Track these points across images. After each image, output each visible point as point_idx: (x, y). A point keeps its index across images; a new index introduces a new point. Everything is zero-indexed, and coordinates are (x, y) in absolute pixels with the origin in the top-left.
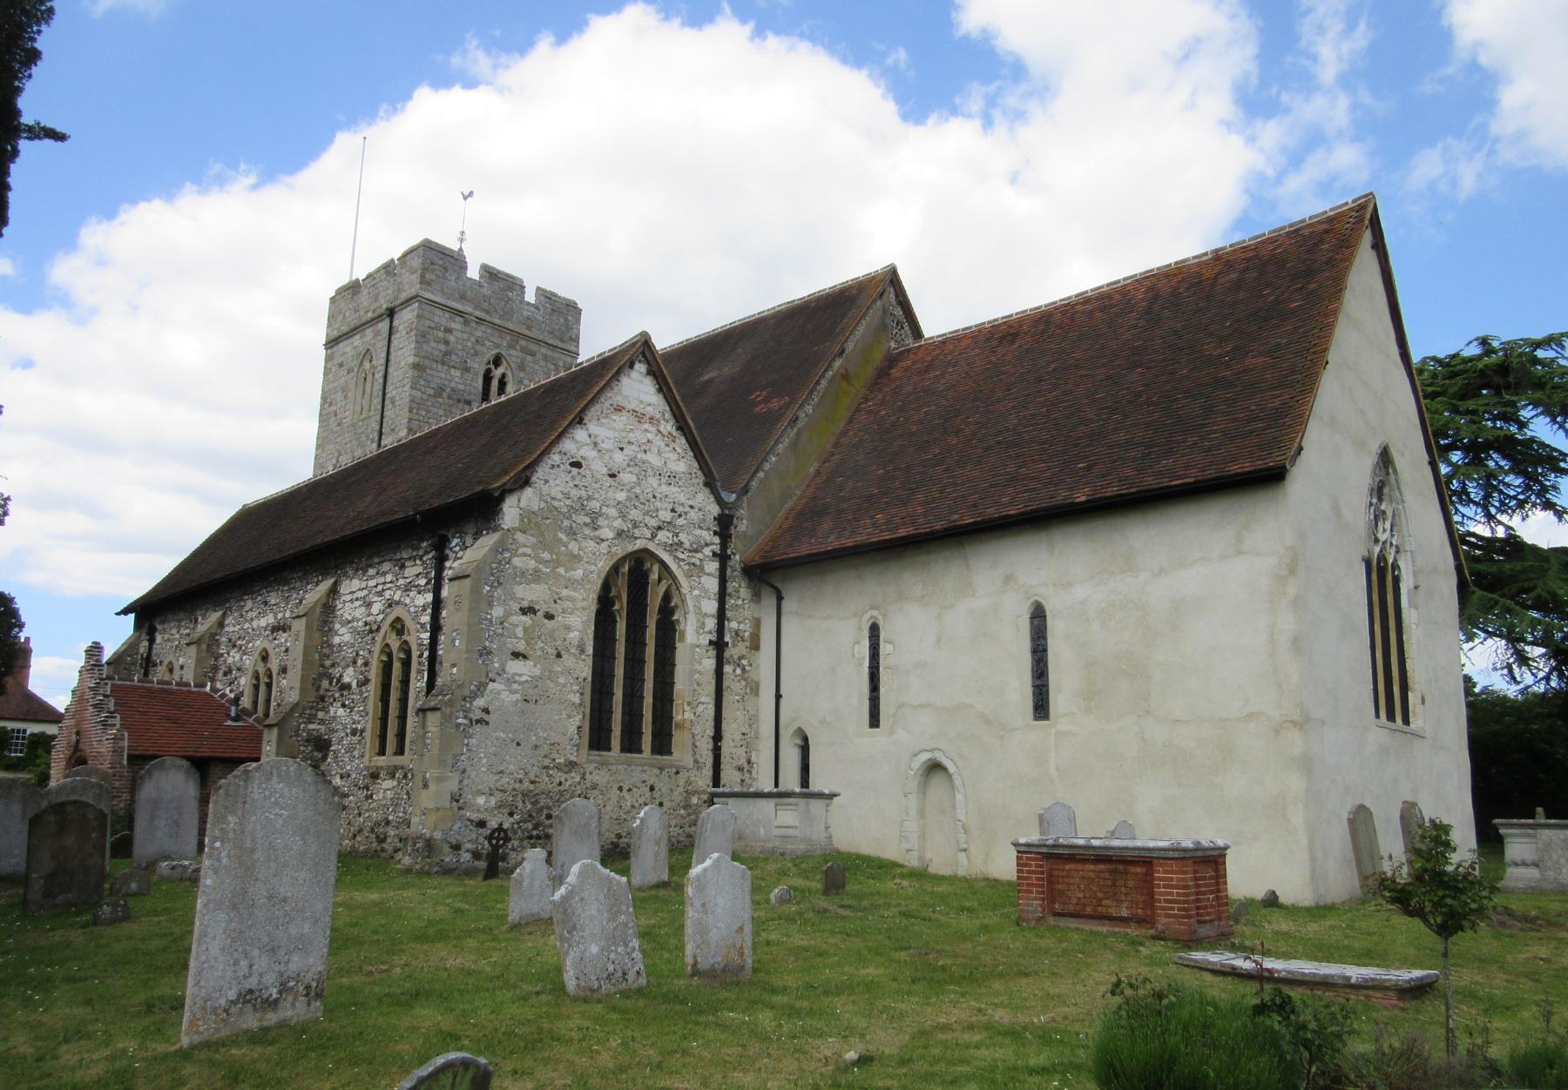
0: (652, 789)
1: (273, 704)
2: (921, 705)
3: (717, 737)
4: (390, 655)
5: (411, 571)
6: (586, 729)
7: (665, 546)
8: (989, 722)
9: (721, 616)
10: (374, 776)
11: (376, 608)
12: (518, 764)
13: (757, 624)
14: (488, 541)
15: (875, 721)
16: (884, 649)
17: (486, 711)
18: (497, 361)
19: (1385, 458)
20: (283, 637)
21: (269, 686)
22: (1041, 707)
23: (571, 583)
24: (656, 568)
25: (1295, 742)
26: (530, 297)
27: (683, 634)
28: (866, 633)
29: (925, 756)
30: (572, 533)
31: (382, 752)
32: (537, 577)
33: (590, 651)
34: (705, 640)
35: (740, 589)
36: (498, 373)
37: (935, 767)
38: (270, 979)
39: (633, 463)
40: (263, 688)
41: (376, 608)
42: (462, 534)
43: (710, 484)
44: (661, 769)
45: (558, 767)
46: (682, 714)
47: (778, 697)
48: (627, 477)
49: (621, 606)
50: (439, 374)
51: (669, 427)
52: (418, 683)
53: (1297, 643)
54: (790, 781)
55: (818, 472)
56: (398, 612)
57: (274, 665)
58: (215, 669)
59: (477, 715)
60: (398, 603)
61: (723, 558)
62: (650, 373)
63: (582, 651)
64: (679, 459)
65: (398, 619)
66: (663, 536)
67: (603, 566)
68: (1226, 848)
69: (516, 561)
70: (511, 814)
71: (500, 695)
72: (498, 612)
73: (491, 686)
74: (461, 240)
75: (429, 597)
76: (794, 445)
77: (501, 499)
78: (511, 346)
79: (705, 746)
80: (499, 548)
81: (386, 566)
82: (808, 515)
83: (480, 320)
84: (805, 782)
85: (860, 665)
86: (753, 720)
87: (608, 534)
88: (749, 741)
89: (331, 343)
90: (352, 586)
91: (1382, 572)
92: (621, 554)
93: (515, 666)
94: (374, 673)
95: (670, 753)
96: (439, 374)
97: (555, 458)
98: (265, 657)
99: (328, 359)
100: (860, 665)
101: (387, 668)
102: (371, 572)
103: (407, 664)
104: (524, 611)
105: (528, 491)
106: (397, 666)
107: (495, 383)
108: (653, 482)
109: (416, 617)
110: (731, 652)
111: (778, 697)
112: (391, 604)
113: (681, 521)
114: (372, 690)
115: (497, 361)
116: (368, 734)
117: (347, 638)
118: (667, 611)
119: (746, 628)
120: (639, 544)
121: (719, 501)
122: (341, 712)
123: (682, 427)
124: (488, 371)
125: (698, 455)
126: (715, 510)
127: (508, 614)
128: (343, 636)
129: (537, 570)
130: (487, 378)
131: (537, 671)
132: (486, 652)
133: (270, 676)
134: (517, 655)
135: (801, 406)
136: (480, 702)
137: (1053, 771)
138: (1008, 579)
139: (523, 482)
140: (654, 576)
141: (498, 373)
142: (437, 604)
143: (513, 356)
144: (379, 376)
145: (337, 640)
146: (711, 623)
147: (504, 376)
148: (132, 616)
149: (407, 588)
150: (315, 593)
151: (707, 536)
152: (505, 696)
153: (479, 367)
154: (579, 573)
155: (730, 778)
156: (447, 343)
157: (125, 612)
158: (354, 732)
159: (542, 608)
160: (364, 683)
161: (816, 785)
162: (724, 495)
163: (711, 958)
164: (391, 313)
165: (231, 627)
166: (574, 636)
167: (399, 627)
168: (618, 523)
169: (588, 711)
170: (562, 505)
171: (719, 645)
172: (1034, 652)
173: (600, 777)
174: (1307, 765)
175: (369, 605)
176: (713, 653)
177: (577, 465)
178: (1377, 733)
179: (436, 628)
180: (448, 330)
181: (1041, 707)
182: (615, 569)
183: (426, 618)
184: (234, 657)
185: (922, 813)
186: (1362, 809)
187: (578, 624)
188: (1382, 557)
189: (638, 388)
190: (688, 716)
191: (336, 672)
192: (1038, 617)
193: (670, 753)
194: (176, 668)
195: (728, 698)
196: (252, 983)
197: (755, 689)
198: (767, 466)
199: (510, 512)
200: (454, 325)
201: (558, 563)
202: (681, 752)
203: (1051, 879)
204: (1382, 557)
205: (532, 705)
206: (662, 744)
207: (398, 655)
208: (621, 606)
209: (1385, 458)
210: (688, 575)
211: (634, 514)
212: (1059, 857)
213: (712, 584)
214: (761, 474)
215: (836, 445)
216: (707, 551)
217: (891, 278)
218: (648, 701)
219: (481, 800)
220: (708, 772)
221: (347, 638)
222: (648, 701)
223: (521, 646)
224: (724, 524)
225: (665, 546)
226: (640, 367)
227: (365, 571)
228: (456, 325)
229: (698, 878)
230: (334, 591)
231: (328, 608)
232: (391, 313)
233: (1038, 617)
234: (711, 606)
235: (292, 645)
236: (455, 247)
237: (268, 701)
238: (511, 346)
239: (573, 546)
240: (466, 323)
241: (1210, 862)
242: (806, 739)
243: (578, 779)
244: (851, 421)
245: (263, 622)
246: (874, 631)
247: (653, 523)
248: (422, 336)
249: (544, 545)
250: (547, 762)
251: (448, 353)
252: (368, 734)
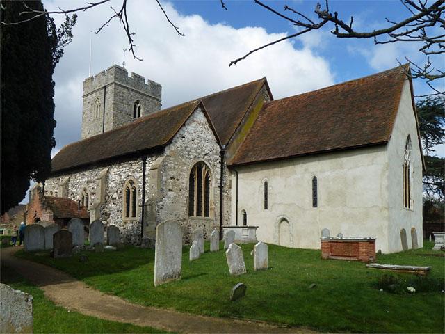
1: (89, 203)
3: (221, 212)
4: (129, 190)
5: (134, 167)
7: (209, 161)
8: (300, 208)
9: (222, 179)
13: (231, 181)
14: (160, 159)
15: (266, 208)
18: (138, 102)
19: (409, 138)
20: (91, 184)
21: (87, 198)
22: (315, 204)
25: (386, 213)
26: (147, 83)
29: (281, 217)
30: (183, 156)
31: (128, 216)
34: (217, 186)
35: (226, 171)
37: (284, 220)
38: (171, 271)
39: (198, 137)
40: (85, 199)
41: (123, 177)
42: (151, 156)
43: (218, 143)
45: (181, 220)
46: (211, 206)
47: (237, 201)
48: (197, 141)
49: (196, 176)
51: (207, 126)
52: (139, 198)
53: (388, 188)
54: (241, 223)
55: (246, 139)
56: (131, 178)
57: (89, 193)
58: (68, 193)
61: (222, 163)
64: (210, 136)
65: (131, 180)
67: (191, 165)
68: (375, 240)
72: (164, 178)
75: (142, 174)
77: (165, 147)
79: (218, 214)
80: (164, 161)
81: (126, 165)
83: (133, 90)
84: (245, 223)
85: (262, 193)
86: (230, 207)
87: (192, 157)
88: (229, 213)
89: (84, 96)
91: (406, 168)
93: (169, 193)
97: (178, 136)
98: (85, 190)
99: (84, 100)
100: (262, 193)
101: (128, 194)
102: (121, 167)
103: (135, 192)
104: (171, 178)
106: (131, 193)
109: (137, 180)
110: (225, 189)
111: (237, 201)
113: (211, 153)
114: (124, 199)
115: (138, 102)
116: (123, 212)
117: (114, 185)
118: (207, 178)
119: (228, 182)
120: (200, 160)
121: (221, 147)
123: (211, 127)
125: (215, 134)
126: (220, 150)
128: (112, 184)
131: (175, 195)
132: (162, 190)
133: (88, 195)
134: (170, 190)
136: (161, 203)
137: (318, 220)
138: (306, 170)
139: (170, 142)
140: (204, 168)
142: (144, 176)
143: (142, 101)
144: (102, 106)
146: (219, 181)
149: (133, 172)
150: (102, 172)
151: (218, 157)
153: (132, 104)
155: (225, 223)
158: (118, 211)
159: (176, 178)
161: (248, 225)
163: (261, 266)
164: (105, 87)
165: (72, 181)
166: (184, 185)
167: (131, 182)
168: (195, 154)
170: (180, 149)
171: (221, 187)
172: (313, 189)
173: (191, 223)
174: (389, 219)
175: (121, 176)
176: (219, 189)
177: (184, 137)
178: (403, 210)
179: (144, 183)
180: (123, 93)
181: (315, 204)
182: (194, 166)
183: (141, 180)
184: (74, 190)
185: (279, 232)
186: (404, 229)
187: (185, 182)
188: (406, 164)
189: (199, 116)
191: (111, 194)
192: (315, 180)
194: (54, 193)
195: (224, 202)
196: (168, 272)
197: (230, 199)
199: (167, 152)
201: (179, 165)
202: (211, 216)
203: (331, 246)
204: (406, 164)
206: (207, 214)
207: (131, 190)
209: (409, 138)
210: (213, 168)
212: (333, 242)
213: (219, 170)
216: (218, 161)
217: (264, 83)
218: (203, 202)
220: (219, 221)
222: (203, 202)
223: (171, 188)
224: (222, 154)
225: (209, 161)
226: (199, 109)
227: (118, 166)
228: (126, 91)
229: (257, 247)
230: (108, 172)
231: (107, 176)
232: (105, 87)
233: (315, 180)
234: (219, 176)
235: (97, 187)
237: (87, 202)
241: (372, 242)
242: (245, 212)
245: (84, 180)
246: (266, 183)
247: (204, 153)
248: (116, 95)
249: (176, 160)
250: (178, 219)
251: (123, 100)
252: (123, 212)
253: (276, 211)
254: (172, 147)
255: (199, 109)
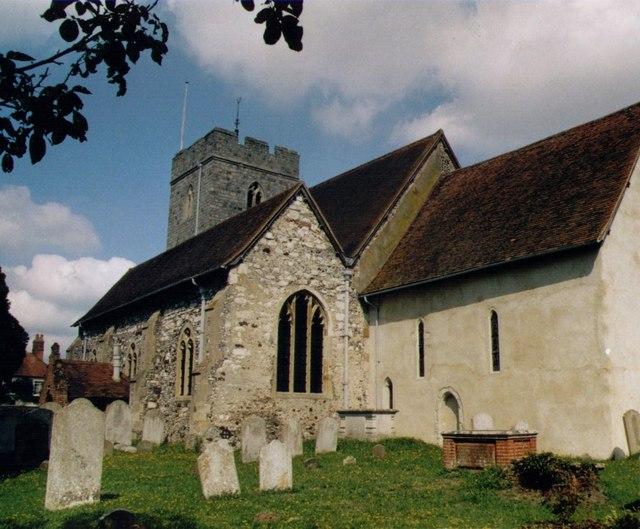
0: (311, 410)
2: (442, 365)
4: (184, 346)
6: (275, 380)
7: (319, 288)
10: (179, 406)
11: (179, 323)
12: (239, 399)
15: (422, 373)
16: (426, 336)
17: (223, 374)
18: (256, 185)
23: (265, 309)
24: (311, 298)
26: (272, 151)
27: (326, 331)
28: (417, 328)
29: (444, 391)
30: (265, 284)
32: (247, 306)
33: (276, 341)
36: (256, 192)
41: (179, 323)
44: (316, 400)
45: (260, 400)
49: (292, 319)
50: (225, 195)
51: (315, 227)
56: (187, 325)
59: (219, 376)
60: (187, 321)
62: (305, 201)
63: (272, 342)
65: (187, 329)
66: (313, 282)
67: (282, 299)
69: (237, 300)
70: (237, 423)
71: (229, 366)
72: (228, 325)
73: (226, 361)
74: (237, 124)
76: (386, 231)
78: (262, 178)
82: (390, 268)
83: (245, 166)
90: (170, 315)
92: (291, 293)
93: (237, 352)
94: (179, 352)
95: (320, 391)
96: (225, 195)
98: (133, 346)
99: (173, 190)
104: (241, 324)
105: (242, 266)
107: (254, 197)
108: (308, 255)
112: (185, 321)
114: (179, 363)
115: (256, 185)
117: (167, 338)
118: (317, 320)
120: (301, 288)
122: (165, 374)
124: (251, 192)
125: (331, 240)
127: (233, 326)
129: (247, 304)
130: (250, 195)
131: (249, 353)
132: (222, 345)
134: (238, 346)
135: (390, 211)
136: (220, 370)
140: (310, 303)
141: (256, 192)
143: (264, 183)
145: (163, 339)
147: (259, 193)
148: (77, 328)
152: (234, 367)
153: (245, 190)
154: (269, 304)
156: (228, 179)
157: (75, 325)
159: (251, 322)
160: (174, 360)
161: (395, 408)
162: (346, 259)
166: (267, 335)
168: (290, 278)
169: (276, 372)
173: (282, 405)
182: (289, 300)
187: (270, 329)
189: (299, 208)
190: (330, 372)
192: (495, 317)
193: (320, 391)
198: (371, 243)
200: (231, 170)
205: (246, 370)
206: (317, 387)
208: (292, 319)
210: (328, 301)
211: (300, 273)
214: (368, 247)
215: (411, 229)
219: (221, 417)
221: (167, 338)
223: (240, 342)
225: (319, 288)
226: (300, 198)
228: (233, 169)
233: (495, 317)
236: (231, 129)
238: (262, 178)
239: (266, 291)
240: (238, 168)
243: (271, 406)
244: (419, 215)
247: (308, 276)
250: (254, 398)
251: (228, 185)
253: (439, 379)
254: (243, 268)
255: (300, 198)
